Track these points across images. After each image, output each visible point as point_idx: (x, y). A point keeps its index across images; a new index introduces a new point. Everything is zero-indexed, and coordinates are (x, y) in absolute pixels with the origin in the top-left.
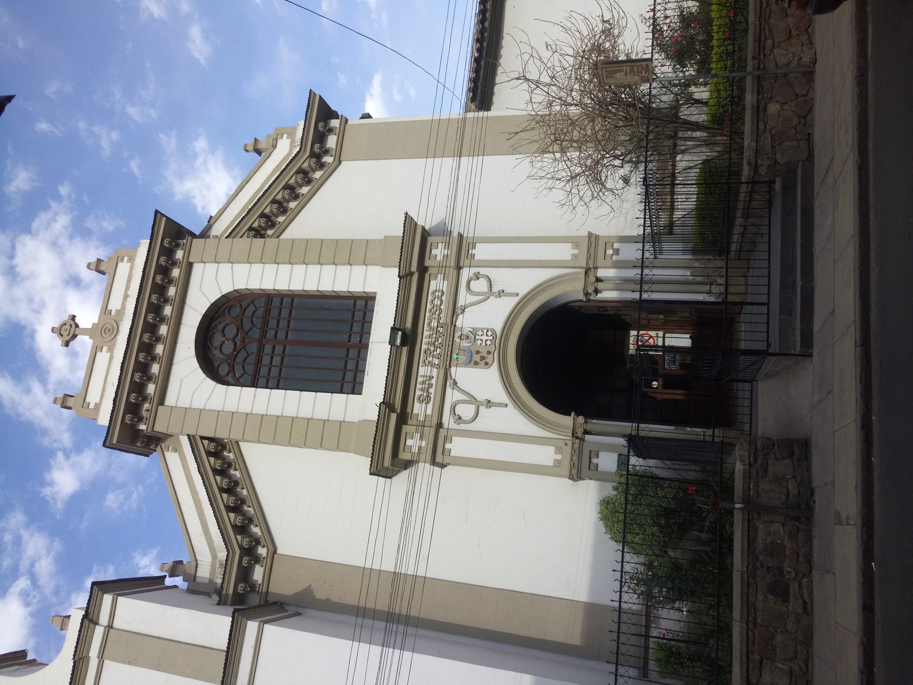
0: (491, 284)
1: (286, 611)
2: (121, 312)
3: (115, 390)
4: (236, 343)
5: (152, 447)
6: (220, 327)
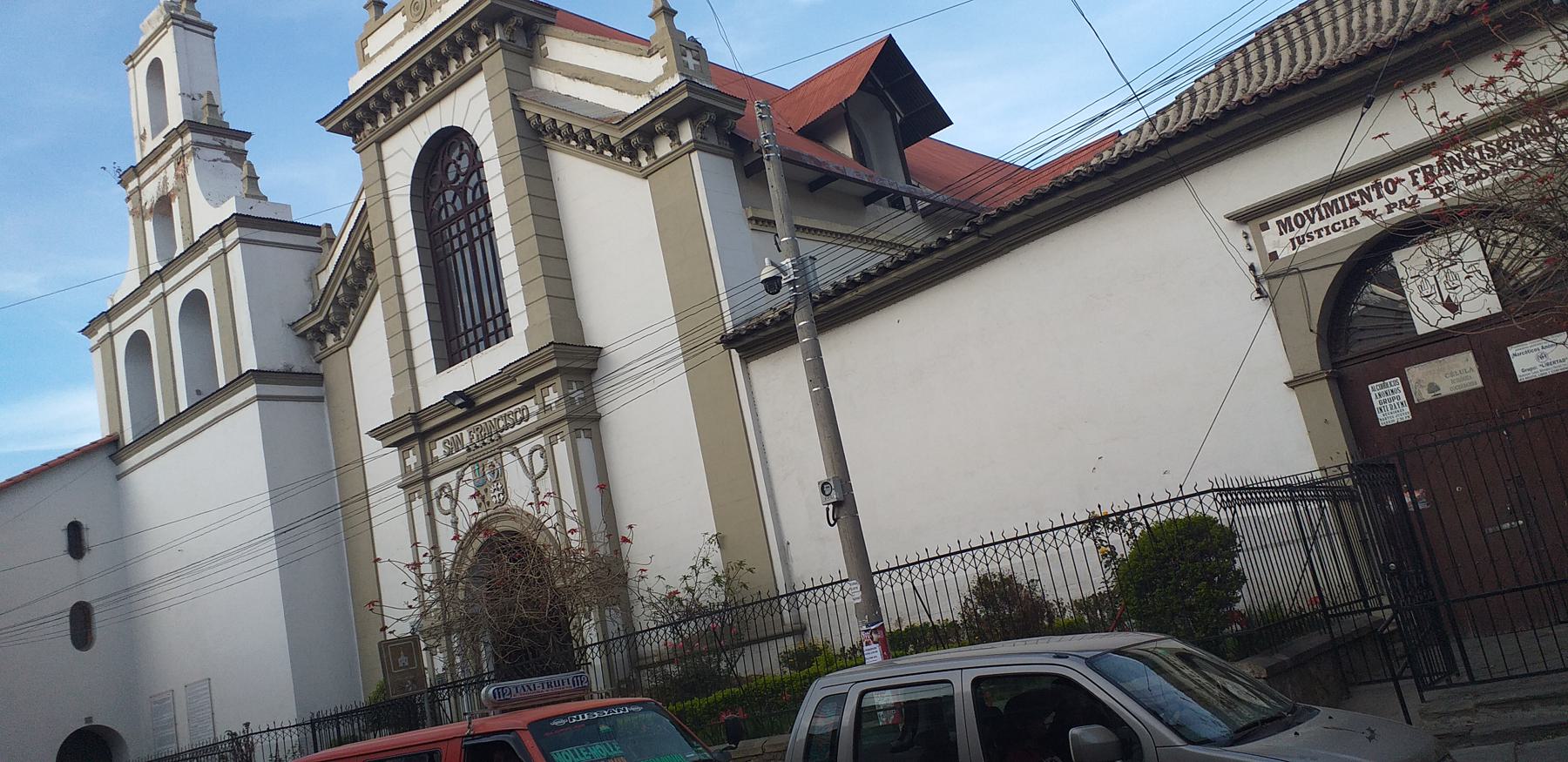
1: (322, 386)
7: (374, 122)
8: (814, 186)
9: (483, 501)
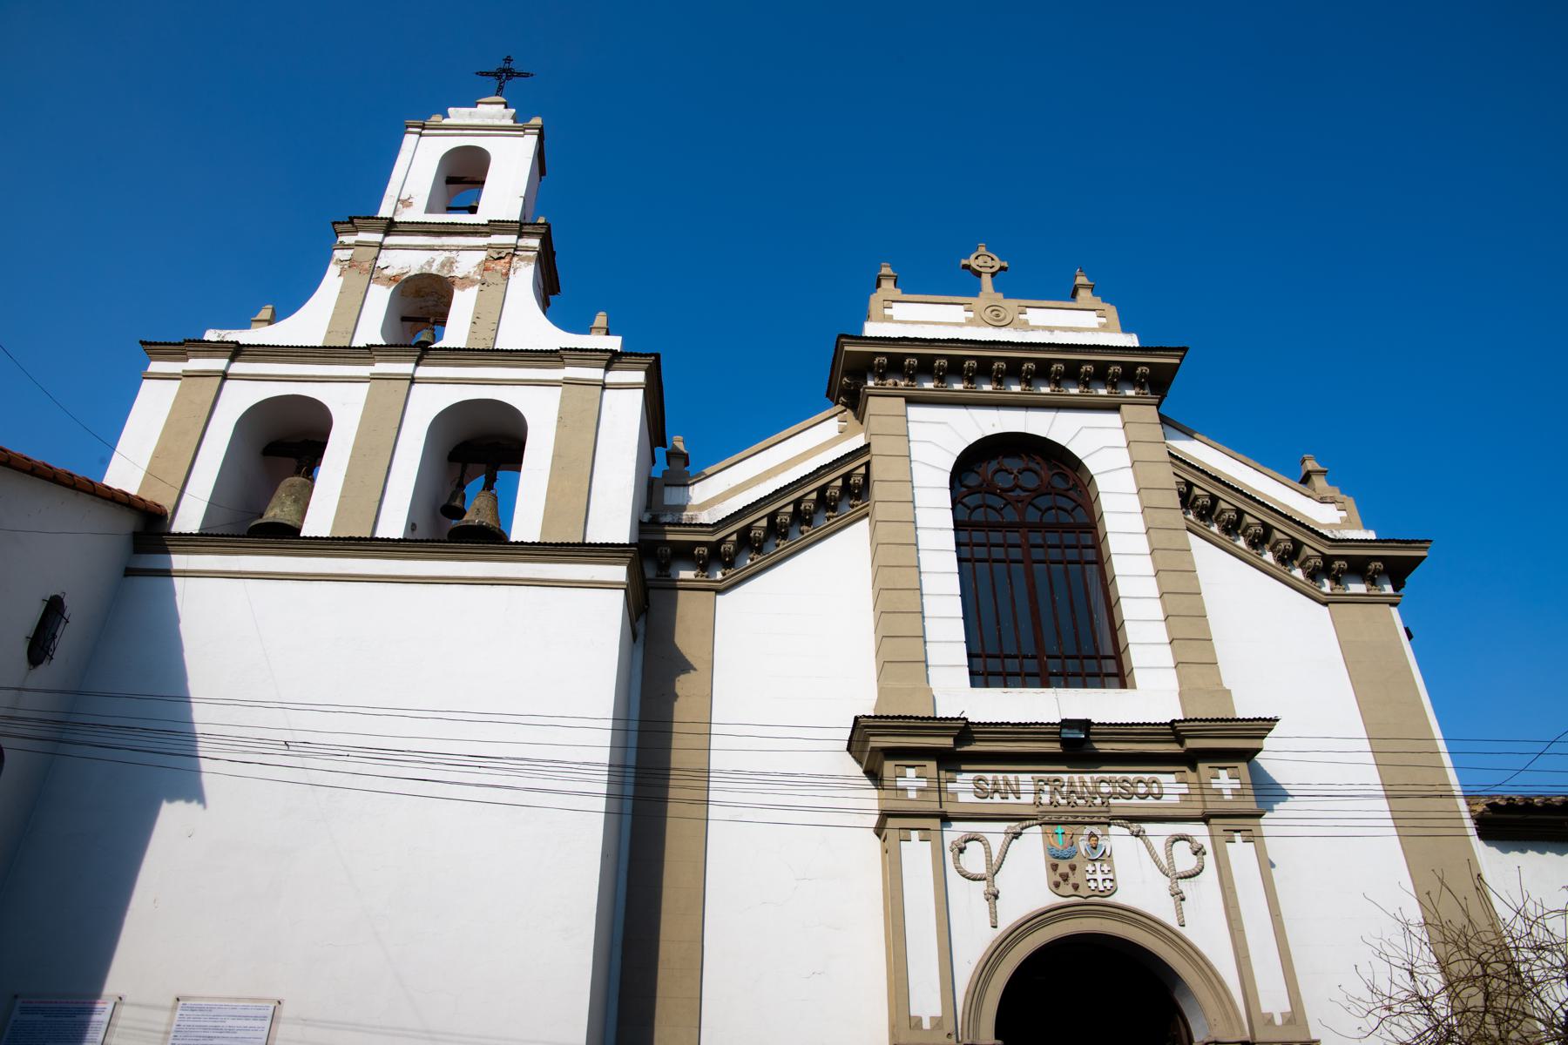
0: (1190, 877)
2: (1025, 326)
3: (919, 337)
4: (1011, 490)
5: (842, 398)
6: (1032, 465)
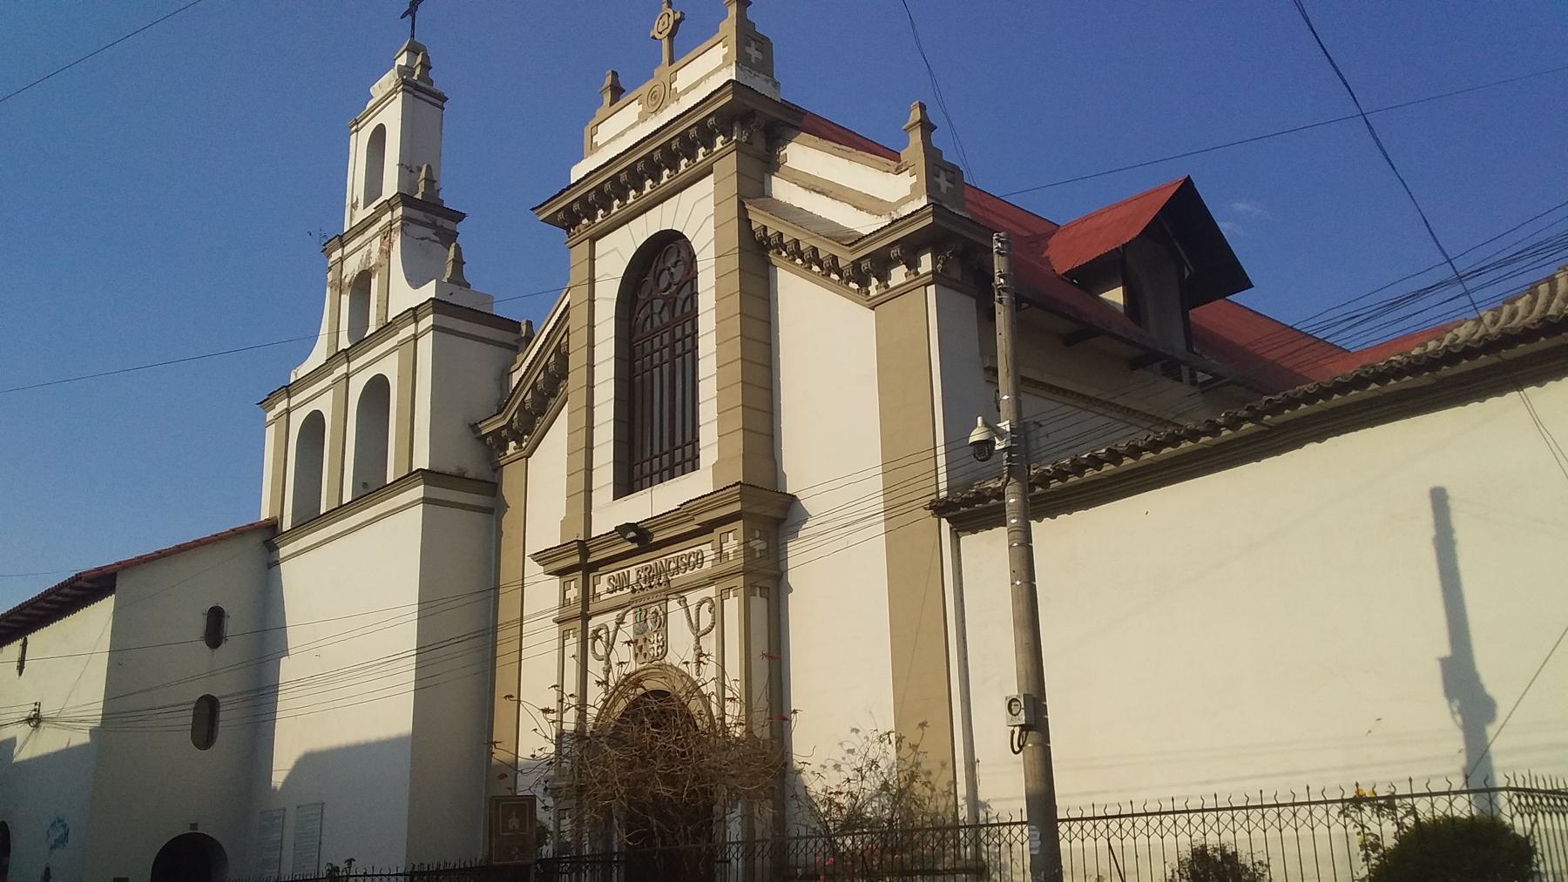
1: (494, 496)
7: (592, 217)
8: (1070, 340)
9: (641, 651)
